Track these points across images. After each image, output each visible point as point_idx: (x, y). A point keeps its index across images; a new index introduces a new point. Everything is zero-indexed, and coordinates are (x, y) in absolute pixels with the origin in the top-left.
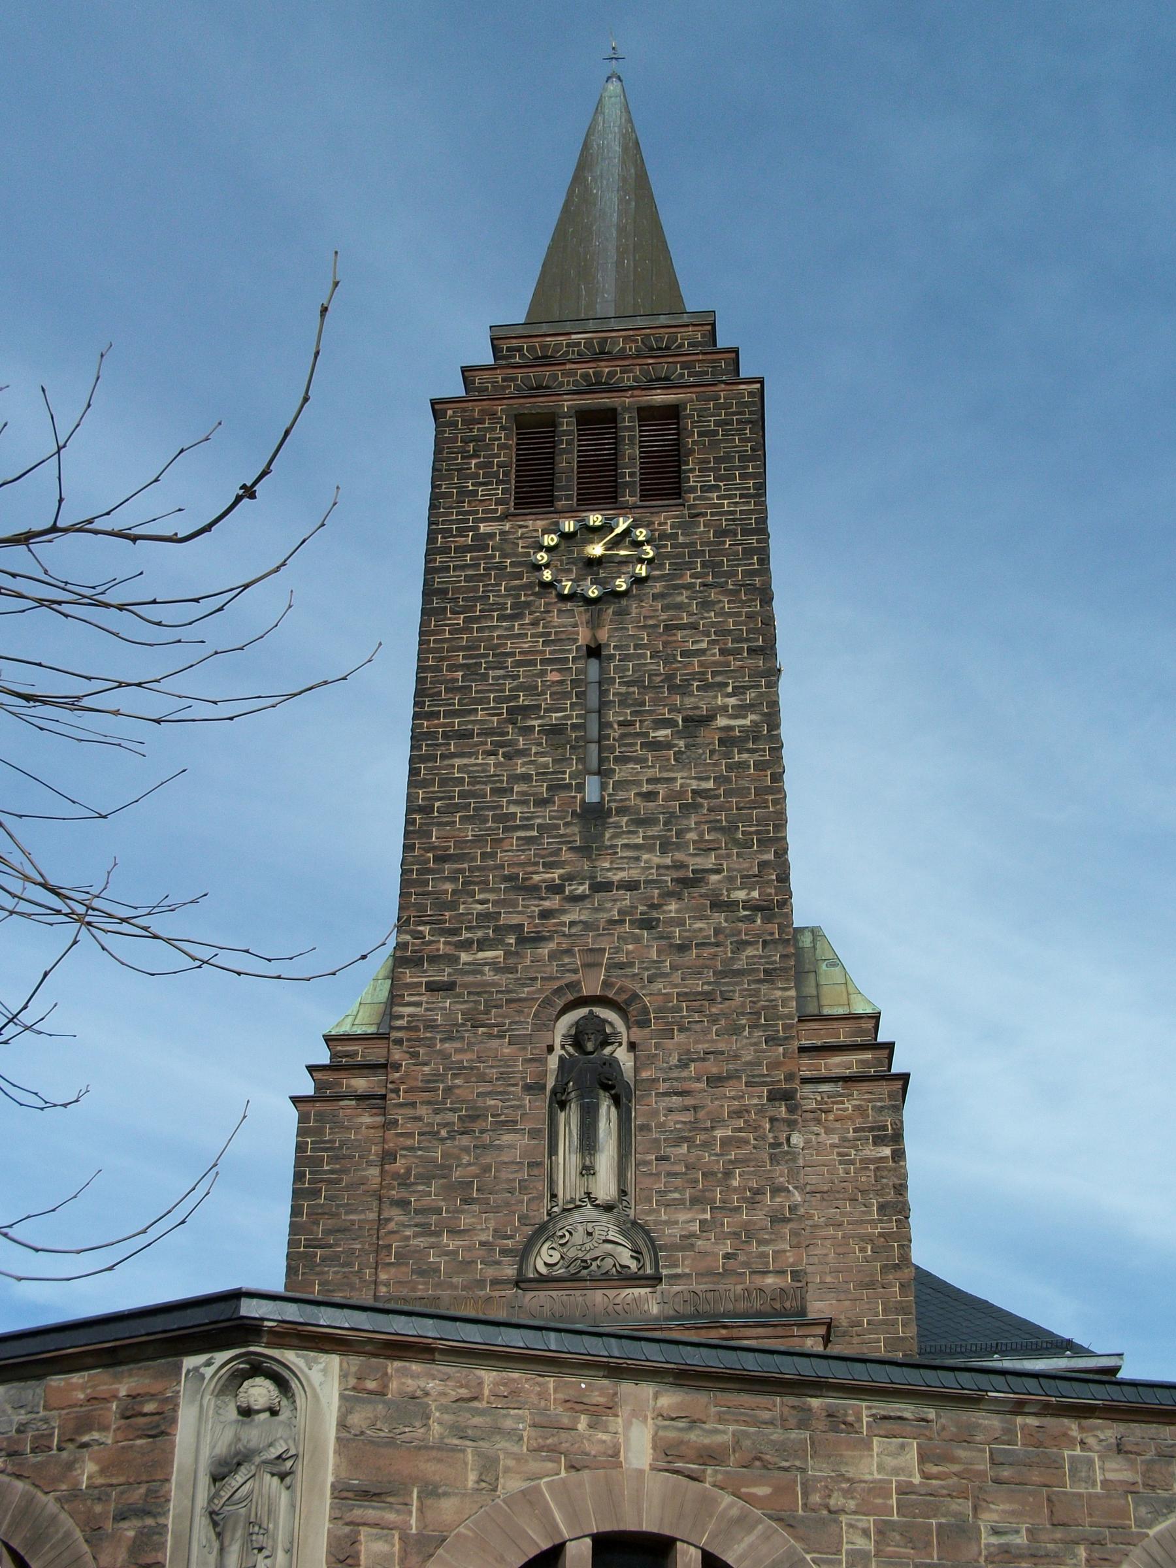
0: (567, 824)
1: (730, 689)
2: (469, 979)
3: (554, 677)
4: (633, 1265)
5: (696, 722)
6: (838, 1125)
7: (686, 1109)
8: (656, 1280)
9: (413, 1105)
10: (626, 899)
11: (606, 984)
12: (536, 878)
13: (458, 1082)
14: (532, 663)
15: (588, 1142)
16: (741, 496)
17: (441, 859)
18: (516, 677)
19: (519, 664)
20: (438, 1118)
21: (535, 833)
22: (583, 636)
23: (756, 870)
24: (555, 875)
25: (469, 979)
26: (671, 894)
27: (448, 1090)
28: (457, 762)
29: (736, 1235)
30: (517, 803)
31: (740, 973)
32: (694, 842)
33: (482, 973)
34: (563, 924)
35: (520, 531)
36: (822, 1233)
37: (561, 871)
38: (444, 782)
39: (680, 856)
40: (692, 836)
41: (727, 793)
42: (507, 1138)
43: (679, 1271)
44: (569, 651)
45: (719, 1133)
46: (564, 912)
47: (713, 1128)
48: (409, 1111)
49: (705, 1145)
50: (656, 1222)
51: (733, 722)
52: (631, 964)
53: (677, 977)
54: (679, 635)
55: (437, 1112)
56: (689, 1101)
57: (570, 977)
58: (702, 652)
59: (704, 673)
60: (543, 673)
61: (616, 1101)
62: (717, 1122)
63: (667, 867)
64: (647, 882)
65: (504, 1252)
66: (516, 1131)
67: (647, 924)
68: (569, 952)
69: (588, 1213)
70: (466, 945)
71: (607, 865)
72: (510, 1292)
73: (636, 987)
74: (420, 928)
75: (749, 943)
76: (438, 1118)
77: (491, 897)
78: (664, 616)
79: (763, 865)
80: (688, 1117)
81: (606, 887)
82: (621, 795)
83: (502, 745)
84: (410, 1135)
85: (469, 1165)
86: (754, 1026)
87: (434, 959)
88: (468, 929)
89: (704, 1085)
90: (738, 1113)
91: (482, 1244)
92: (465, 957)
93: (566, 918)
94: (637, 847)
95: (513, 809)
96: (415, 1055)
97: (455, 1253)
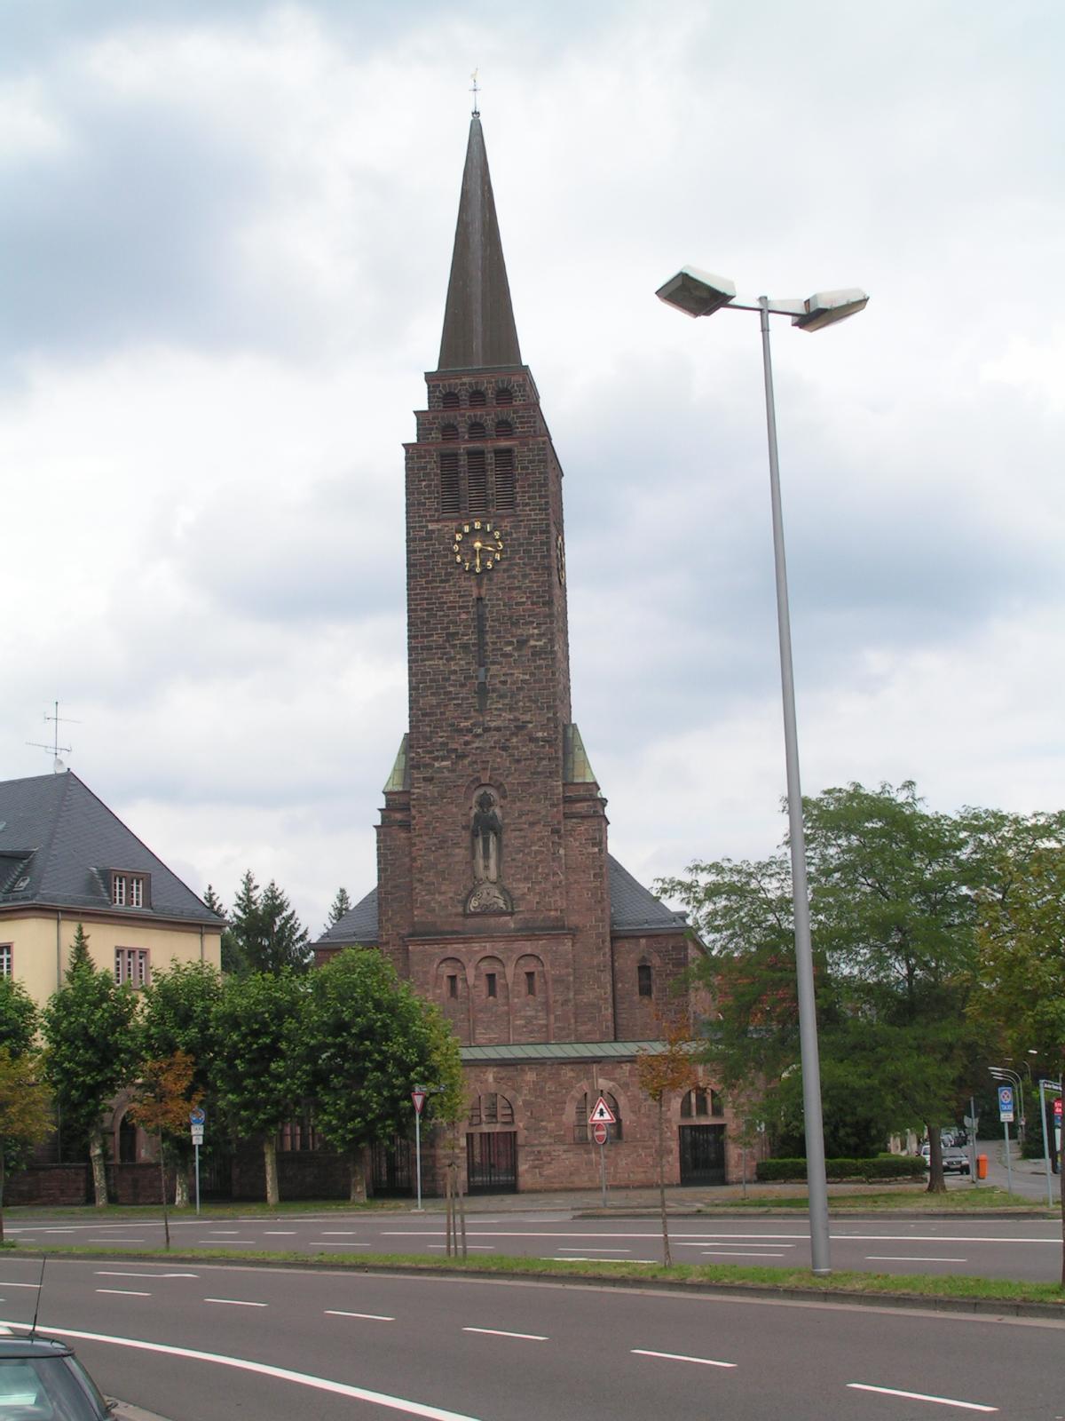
0: (473, 697)
1: (535, 625)
2: (438, 775)
3: (464, 616)
4: (504, 907)
5: (522, 643)
6: (579, 837)
7: (521, 837)
8: (512, 914)
9: (421, 836)
10: (497, 736)
11: (490, 778)
12: (462, 724)
13: (437, 825)
14: (454, 608)
15: (486, 856)
16: (540, 510)
17: (424, 715)
18: (449, 616)
19: (449, 608)
20: (431, 842)
21: (460, 702)
22: (475, 594)
23: (545, 722)
24: (468, 724)
25: (438, 775)
26: (513, 734)
27: (434, 828)
28: (427, 663)
29: (540, 894)
30: (452, 685)
31: (539, 773)
32: (523, 708)
33: (443, 772)
34: (473, 749)
35: (447, 528)
36: (573, 886)
37: (472, 721)
38: (423, 674)
39: (517, 714)
40: (521, 704)
41: (535, 682)
42: (457, 850)
43: (521, 909)
44: (469, 602)
45: (533, 848)
46: (474, 742)
47: (531, 846)
48: (420, 839)
49: (528, 854)
50: (513, 888)
51: (537, 643)
52: (499, 769)
53: (516, 776)
54: (515, 592)
55: (431, 838)
56: (522, 834)
57: (478, 774)
58: (523, 603)
59: (524, 615)
60: (459, 614)
61: (496, 834)
62: (533, 843)
63: (511, 720)
64: (505, 727)
65: (459, 902)
66: (460, 847)
67: (504, 748)
68: (475, 762)
69: (488, 885)
70: (436, 759)
71: (488, 719)
72: (461, 919)
73: (501, 779)
74: (419, 750)
75: (543, 759)
76: (431, 842)
77: (446, 735)
78: (508, 582)
79: (548, 719)
80: (522, 841)
81: (486, 730)
82: (493, 682)
83: (445, 654)
84: (421, 850)
85: (444, 863)
86: (546, 799)
87: (426, 766)
88: (437, 750)
89: (526, 826)
90: (540, 839)
91: (451, 898)
92: (436, 764)
93: (475, 745)
94: (500, 709)
95: (451, 689)
96: (420, 812)
97: (440, 902)
